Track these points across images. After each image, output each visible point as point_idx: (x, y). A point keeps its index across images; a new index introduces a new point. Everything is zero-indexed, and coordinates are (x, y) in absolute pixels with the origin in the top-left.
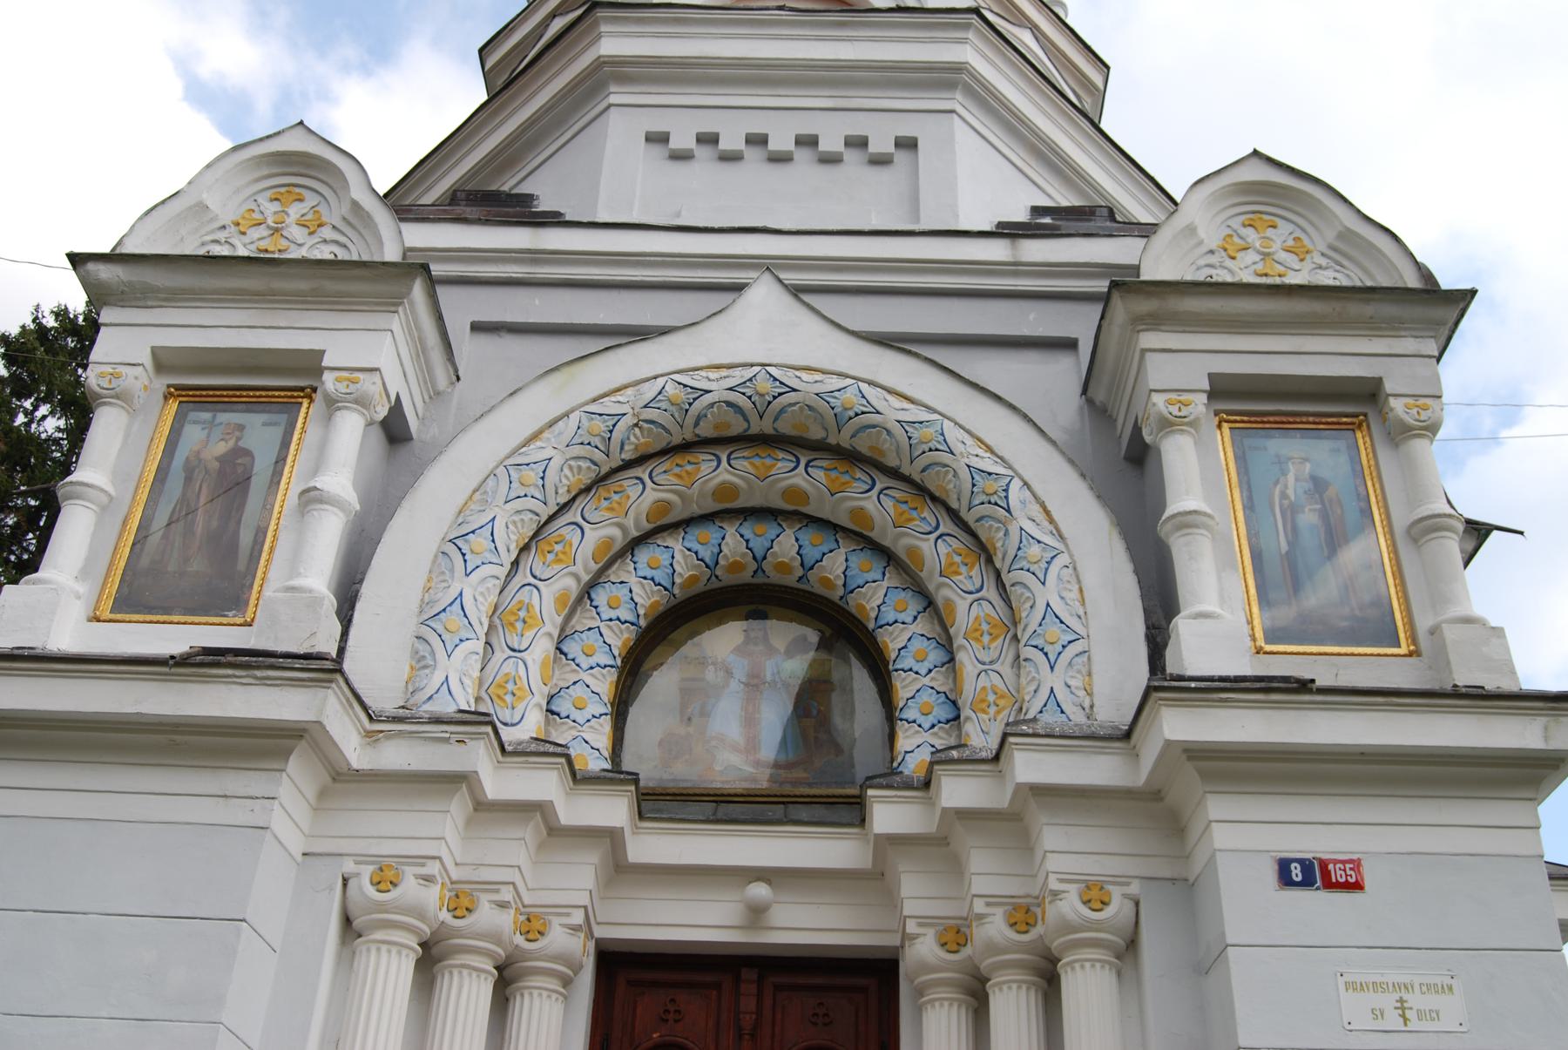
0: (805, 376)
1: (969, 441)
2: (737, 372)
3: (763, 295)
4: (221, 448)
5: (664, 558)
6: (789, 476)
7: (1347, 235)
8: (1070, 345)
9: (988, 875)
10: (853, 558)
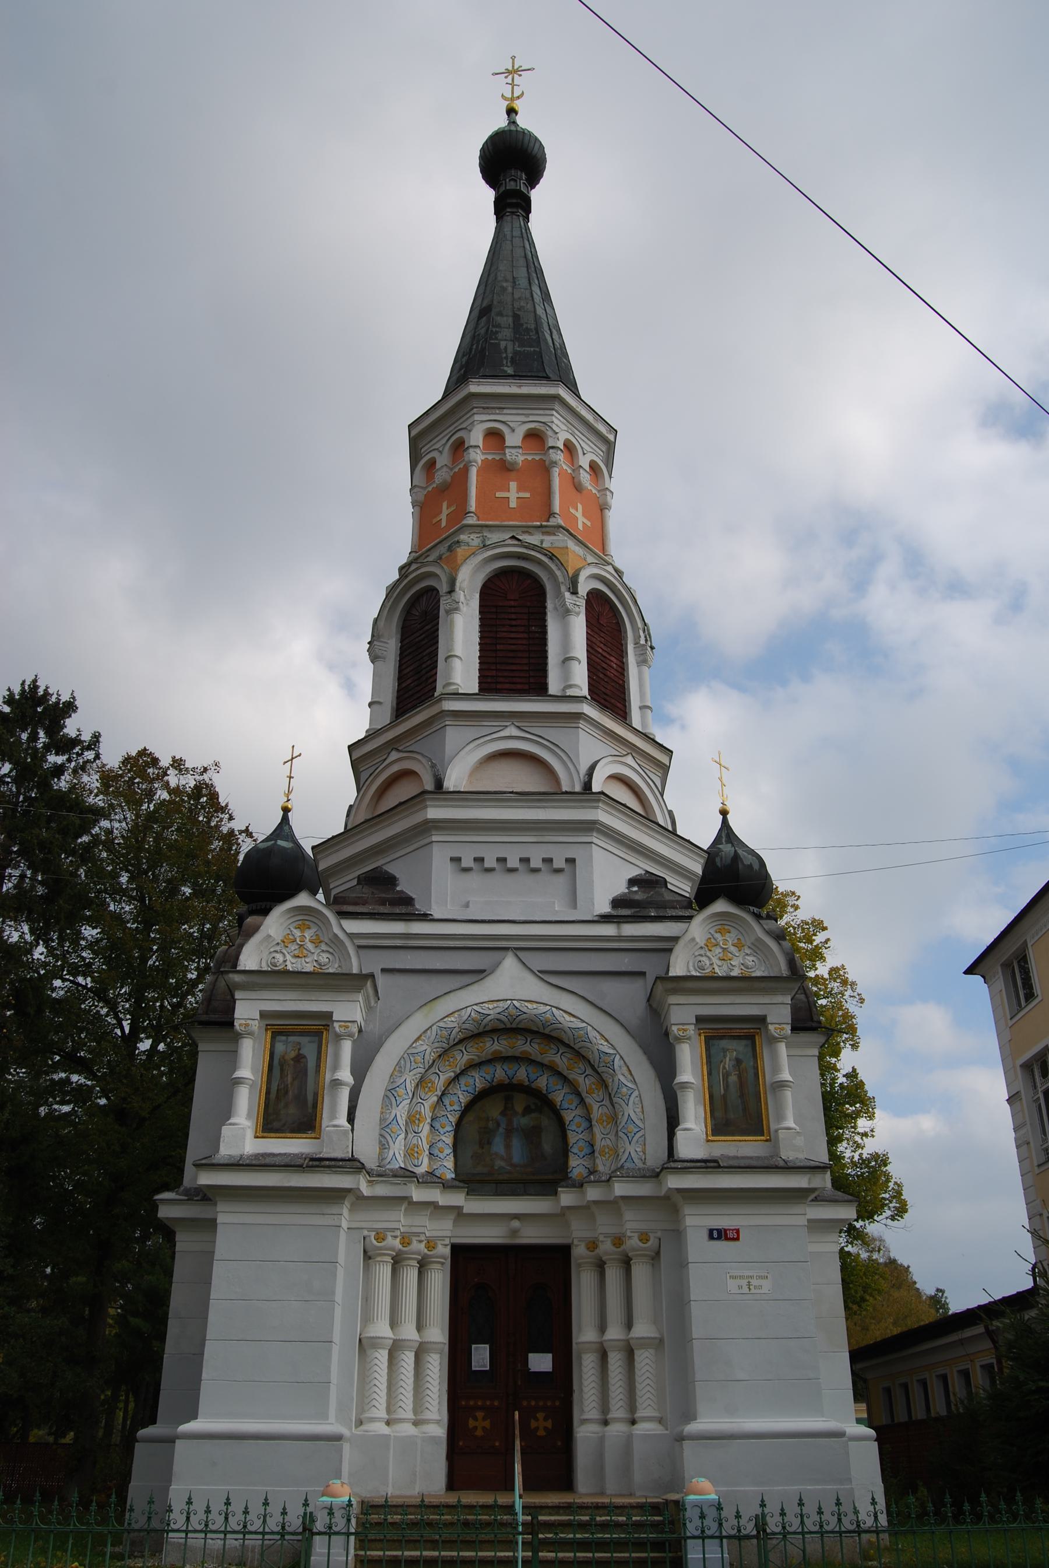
0: (529, 1005)
1: (598, 1037)
2: (501, 1004)
5: (471, 1081)
6: (523, 1046)
8: (642, 974)
10: (550, 1079)
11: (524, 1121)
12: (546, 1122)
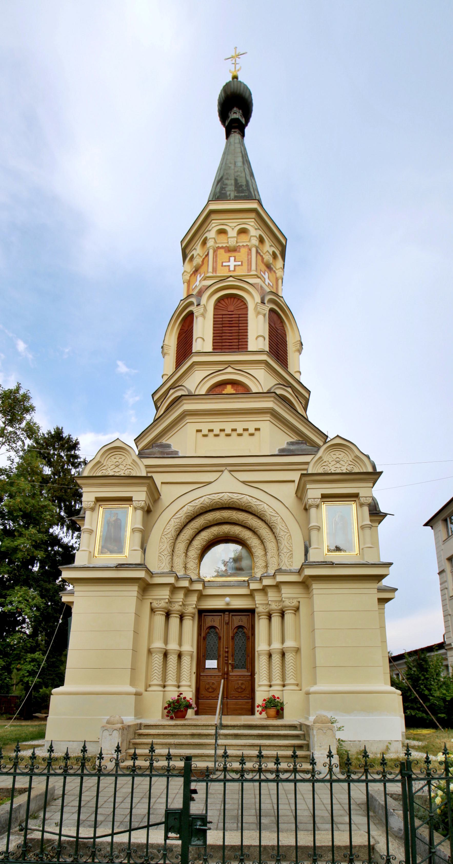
3: (226, 473)
7: (357, 457)
8: (293, 481)
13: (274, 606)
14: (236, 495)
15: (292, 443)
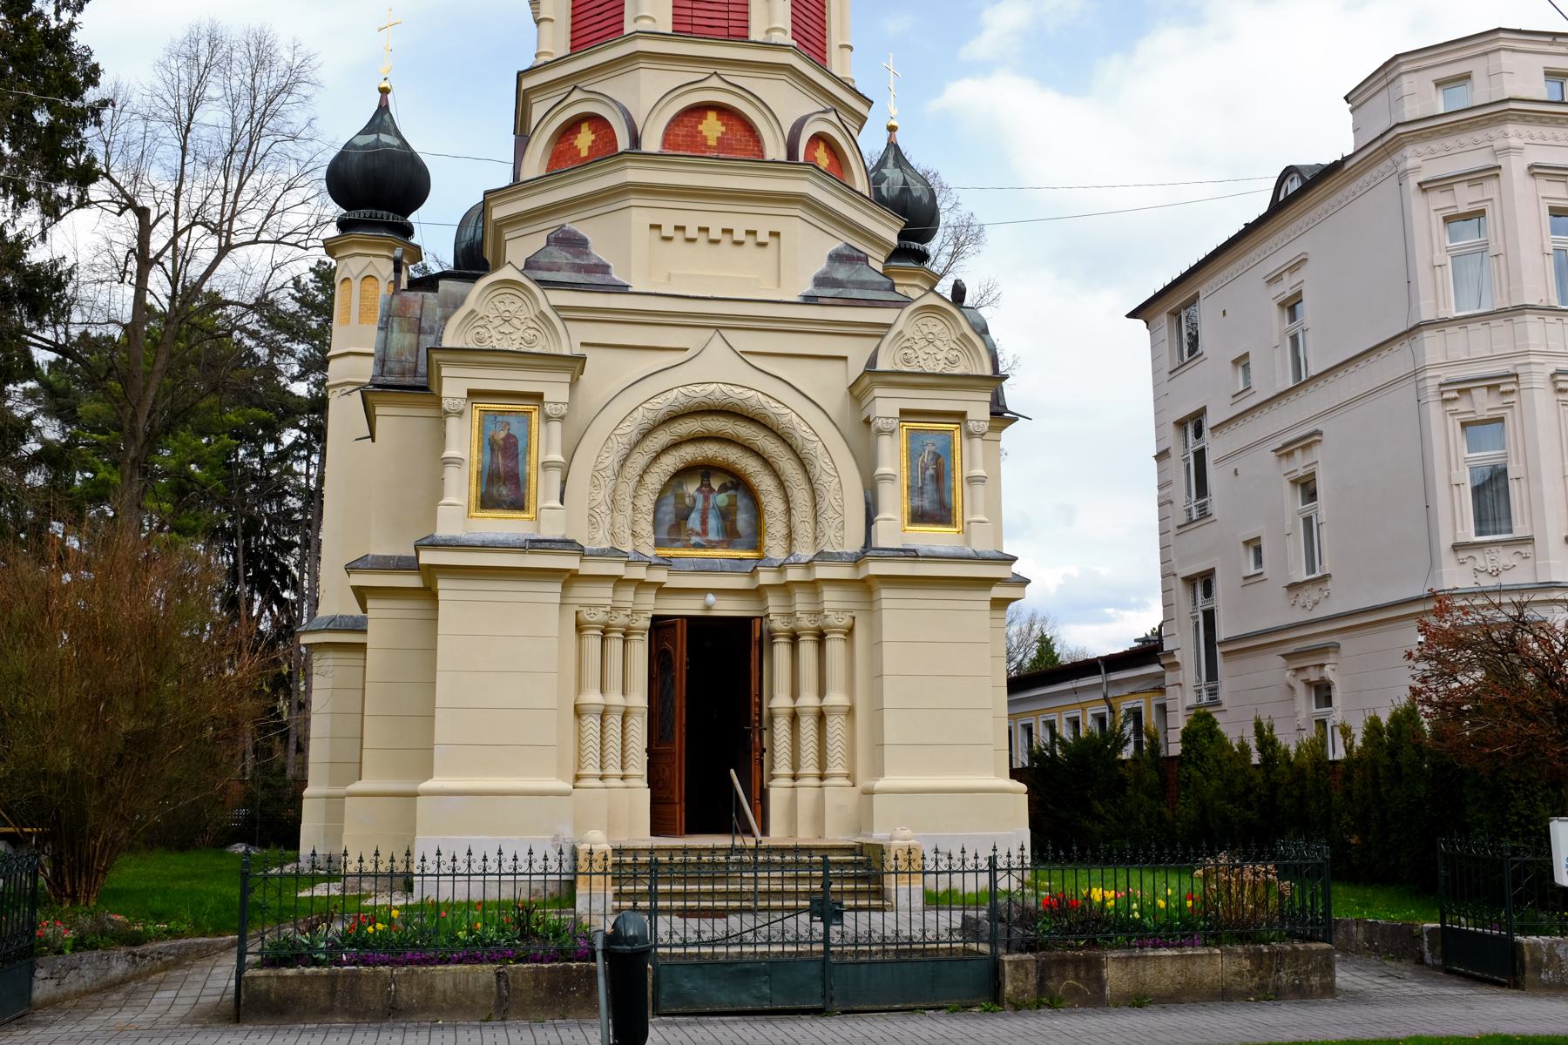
4: (502, 434)
9: (801, 602)
11: (722, 499)
12: (742, 502)
13: (805, 622)
14: (737, 390)
15: (837, 258)
